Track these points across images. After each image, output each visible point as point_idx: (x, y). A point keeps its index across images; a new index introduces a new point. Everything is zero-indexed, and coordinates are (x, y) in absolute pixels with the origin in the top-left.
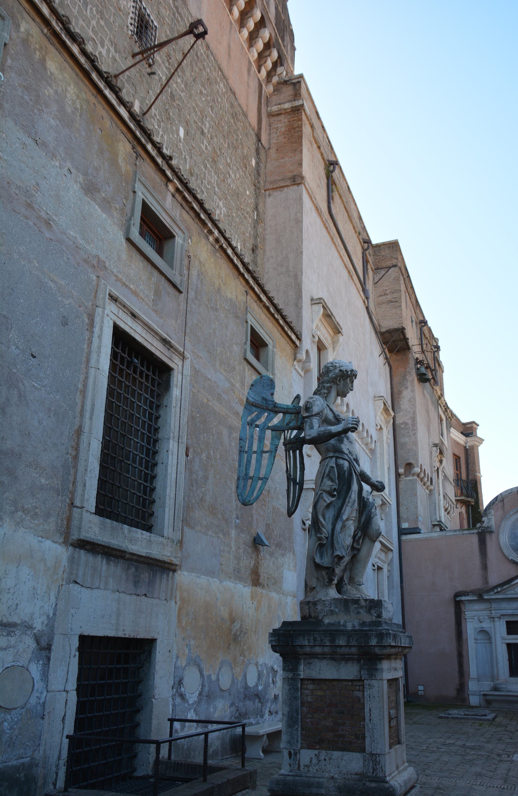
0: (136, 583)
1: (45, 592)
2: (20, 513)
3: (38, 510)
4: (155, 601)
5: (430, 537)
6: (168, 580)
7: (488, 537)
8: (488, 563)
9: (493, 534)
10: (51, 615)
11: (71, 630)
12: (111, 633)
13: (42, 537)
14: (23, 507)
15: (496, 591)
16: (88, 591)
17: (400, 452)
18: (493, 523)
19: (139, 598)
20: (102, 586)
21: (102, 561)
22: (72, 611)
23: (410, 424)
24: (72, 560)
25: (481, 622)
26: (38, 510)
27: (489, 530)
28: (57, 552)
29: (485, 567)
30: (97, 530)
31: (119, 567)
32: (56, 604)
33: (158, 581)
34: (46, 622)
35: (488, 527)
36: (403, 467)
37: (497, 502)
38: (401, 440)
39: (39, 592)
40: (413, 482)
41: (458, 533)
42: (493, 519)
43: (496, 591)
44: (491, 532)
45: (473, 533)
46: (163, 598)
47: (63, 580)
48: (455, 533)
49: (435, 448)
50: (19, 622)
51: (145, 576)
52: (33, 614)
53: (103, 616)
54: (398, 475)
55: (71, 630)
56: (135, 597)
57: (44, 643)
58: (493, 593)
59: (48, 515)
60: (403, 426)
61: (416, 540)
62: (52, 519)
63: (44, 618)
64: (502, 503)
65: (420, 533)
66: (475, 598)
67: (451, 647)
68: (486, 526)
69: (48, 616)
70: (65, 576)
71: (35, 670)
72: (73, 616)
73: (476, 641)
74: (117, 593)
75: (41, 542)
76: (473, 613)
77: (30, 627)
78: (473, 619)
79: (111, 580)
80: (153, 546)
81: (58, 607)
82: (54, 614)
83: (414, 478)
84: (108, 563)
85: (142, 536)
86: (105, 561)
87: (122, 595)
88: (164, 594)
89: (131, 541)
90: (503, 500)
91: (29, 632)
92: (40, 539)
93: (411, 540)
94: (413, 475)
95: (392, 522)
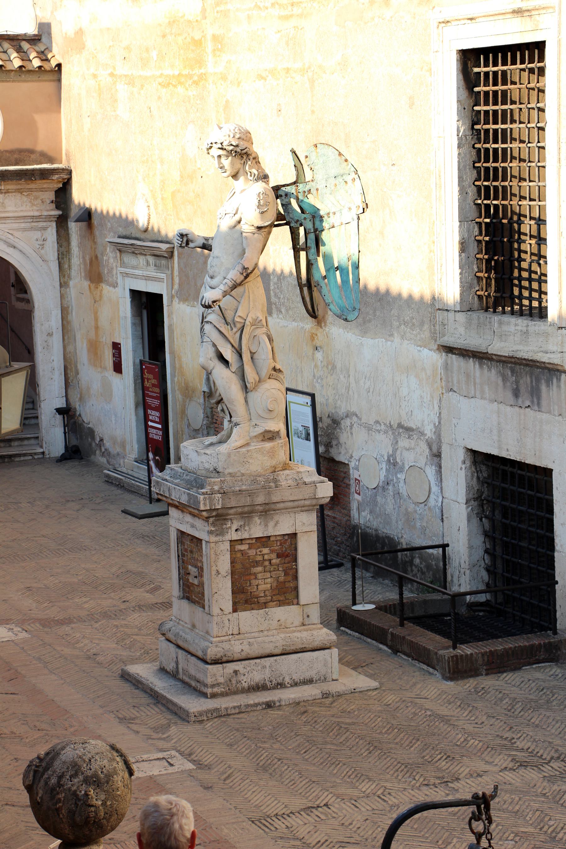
0: (516, 394)
1: (430, 401)
2: (403, 326)
3: (414, 321)
4: (545, 416)
6: (559, 387)
10: (437, 424)
11: (456, 441)
12: (495, 452)
13: (421, 347)
14: (404, 320)
16: (466, 400)
19: (522, 411)
20: (478, 394)
21: (474, 365)
22: (454, 421)
24: (446, 367)
26: (414, 321)
28: (433, 358)
30: (462, 330)
31: (493, 371)
32: (440, 413)
33: (543, 388)
34: (434, 430)
39: (425, 400)
46: (556, 413)
47: (442, 387)
50: (414, 427)
51: (526, 381)
52: (423, 421)
53: (483, 430)
55: (456, 441)
56: (517, 409)
57: (435, 449)
59: (422, 323)
62: (426, 327)
63: (431, 426)
69: (435, 424)
70: (444, 384)
71: (431, 472)
72: (455, 426)
74: (496, 403)
75: (420, 351)
77: (422, 434)
79: (486, 389)
80: (530, 340)
81: (442, 415)
82: (439, 423)
84: (481, 365)
85: (517, 328)
86: (477, 366)
87: (502, 406)
88: (556, 407)
89: (502, 337)
91: (422, 438)
92: (419, 348)
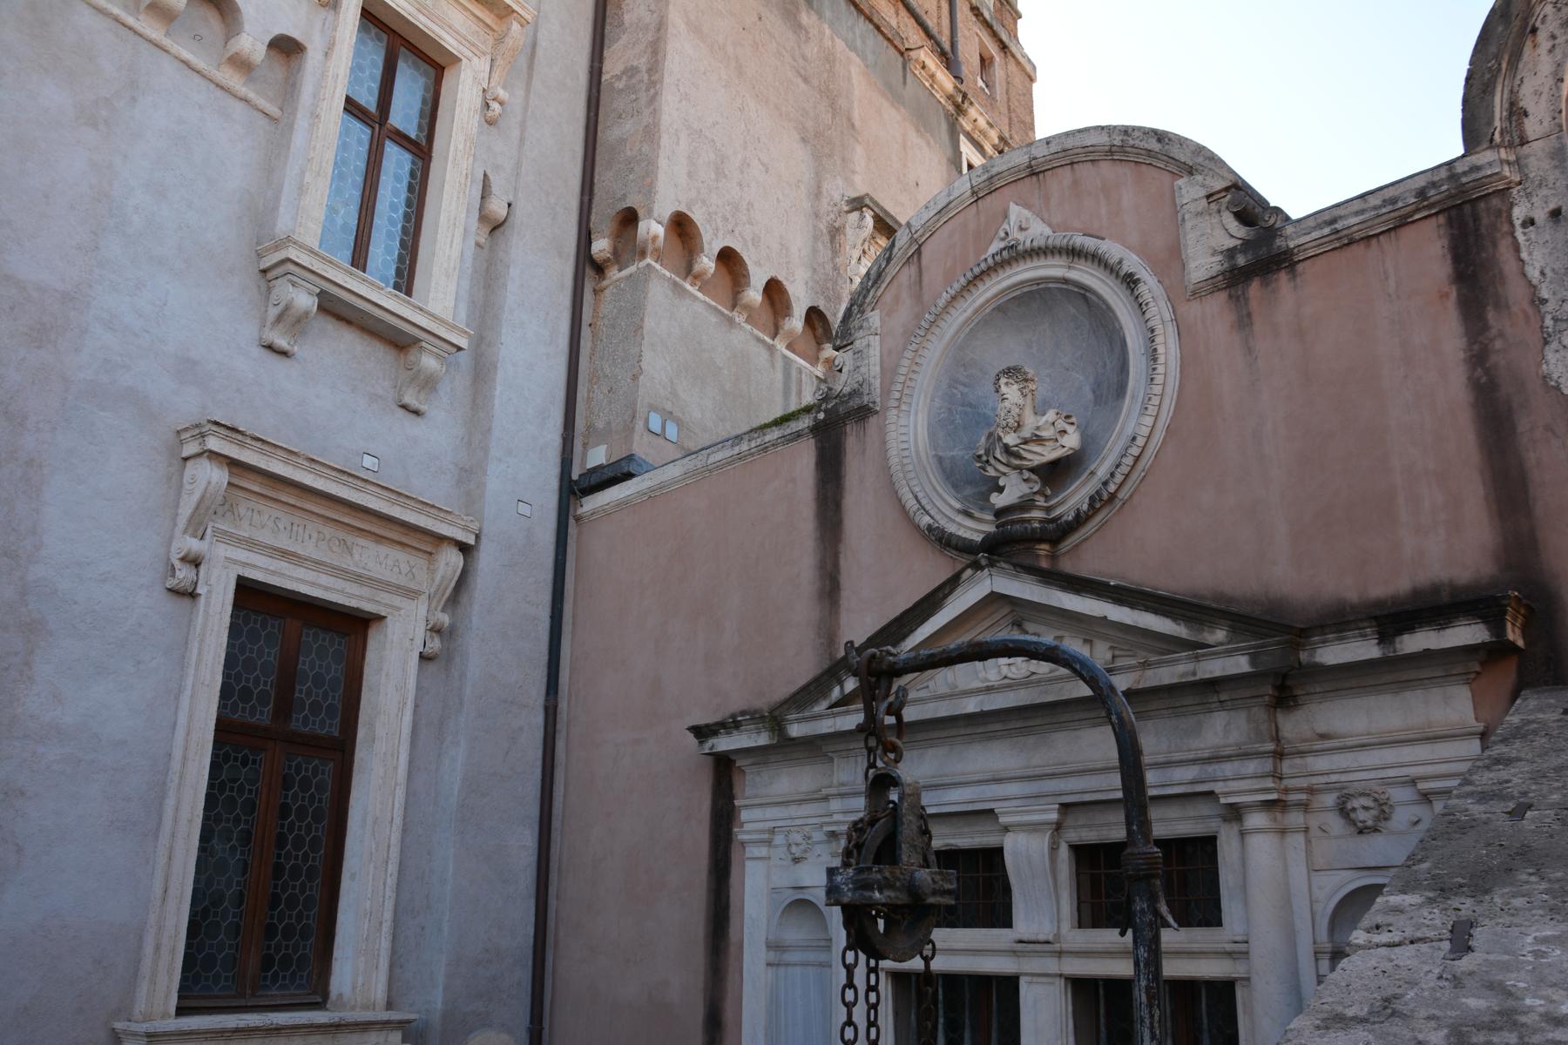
5: (661, 486)
7: (851, 443)
8: (842, 562)
9: (873, 420)
15: (836, 693)
17: (603, 178)
18: (873, 367)
23: (644, 69)
25: (796, 860)
27: (855, 403)
29: (830, 587)
35: (855, 393)
36: (607, 232)
37: (892, 270)
38: (609, 134)
40: (638, 283)
41: (744, 447)
42: (875, 354)
43: (836, 693)
44: (864, 413)
45: (798, 435)
48: (736, 450)
49: (856, 215)
54: (589, 266)
58: (824, 704)
60: (620, 85)
61: (623, 505)
64: (913, 269)
65: (629, 476)
66: (763, 739)
67: (683, 982)
68: (847, 390)
73: (772, 956)
76: (771, 812)
78: (769, 843)
83: (642, 264)
90: (918, 252)
93: (606, 513)
94: (643, 254)
95: (490, 429)
